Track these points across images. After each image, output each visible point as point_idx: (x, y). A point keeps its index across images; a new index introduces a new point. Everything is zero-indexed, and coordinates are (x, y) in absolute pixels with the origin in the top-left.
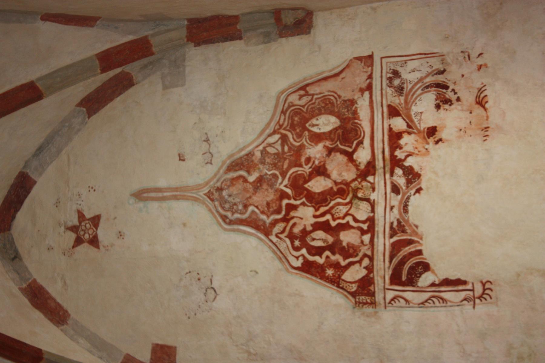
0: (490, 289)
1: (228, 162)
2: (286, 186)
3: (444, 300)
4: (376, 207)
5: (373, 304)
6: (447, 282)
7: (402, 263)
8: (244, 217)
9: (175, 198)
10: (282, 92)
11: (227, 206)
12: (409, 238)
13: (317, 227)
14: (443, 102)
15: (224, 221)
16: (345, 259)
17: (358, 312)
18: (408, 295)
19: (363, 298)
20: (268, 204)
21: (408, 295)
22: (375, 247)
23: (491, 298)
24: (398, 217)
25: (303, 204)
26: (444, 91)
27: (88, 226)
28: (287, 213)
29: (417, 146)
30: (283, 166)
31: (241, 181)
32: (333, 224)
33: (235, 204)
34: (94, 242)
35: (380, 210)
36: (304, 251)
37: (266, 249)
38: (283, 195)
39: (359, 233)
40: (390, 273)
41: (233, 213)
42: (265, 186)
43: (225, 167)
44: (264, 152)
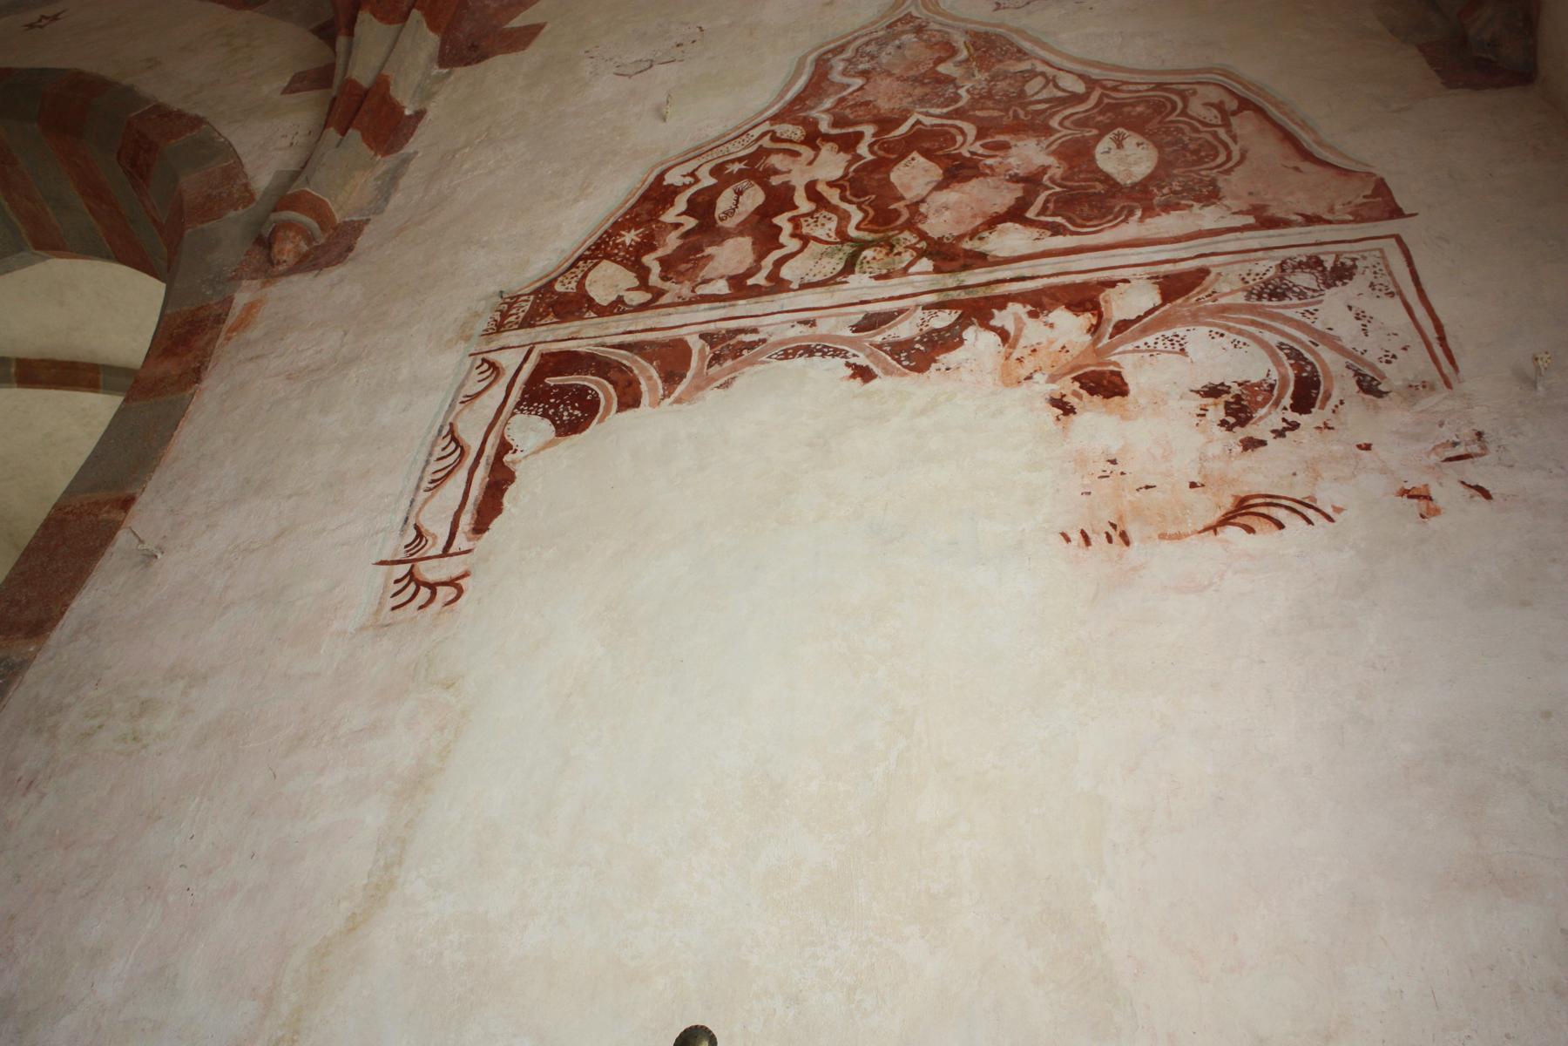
6: (500, 479)
8: (835, 76)
12: (690, 374)
26: (1287, 401)
28: (827, 138)
29: (1042, 354)
30: (982, 109)
36: (708, 181)
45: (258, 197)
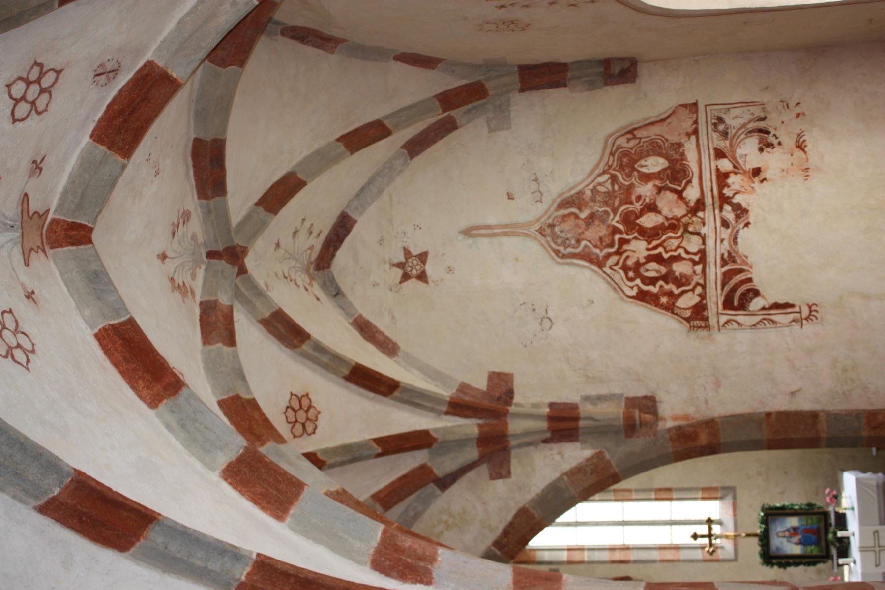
0: (816, 311)
1: (559, 200)
2: (617, 222)
3: (774, 322)
4: (707, 240)
5: (707, 327)
6: (776, 306)
7: (734, 290)
9: (506, 234)
10: (610, 136)
11: (559, 241)
12: (739, 267)
13: (649, 259)
14: (765, 145)
15: (558, 256)
16: (678, 287)
17: (693, 335)
18: (740, 319)
19: (697, 323)
20: (601, 239)
21: (740, 319)
22: (707, 275)
23: (817, 318)
24: (728, 248)
25: (635, 238)
27: (415, 262)
28: (620, 247)
31: (572, 218)
32: (666, 256)
33: (568, 239)
34: (422, 277)
35: (710, 243)
37: (600, 280)
38: (615, 230)
39: (691, 264)
40: (723, 299)
41: (566, 248)
42: (597, 222)
43: (555, 205)
44: (594, 191)
45: (597, 451)
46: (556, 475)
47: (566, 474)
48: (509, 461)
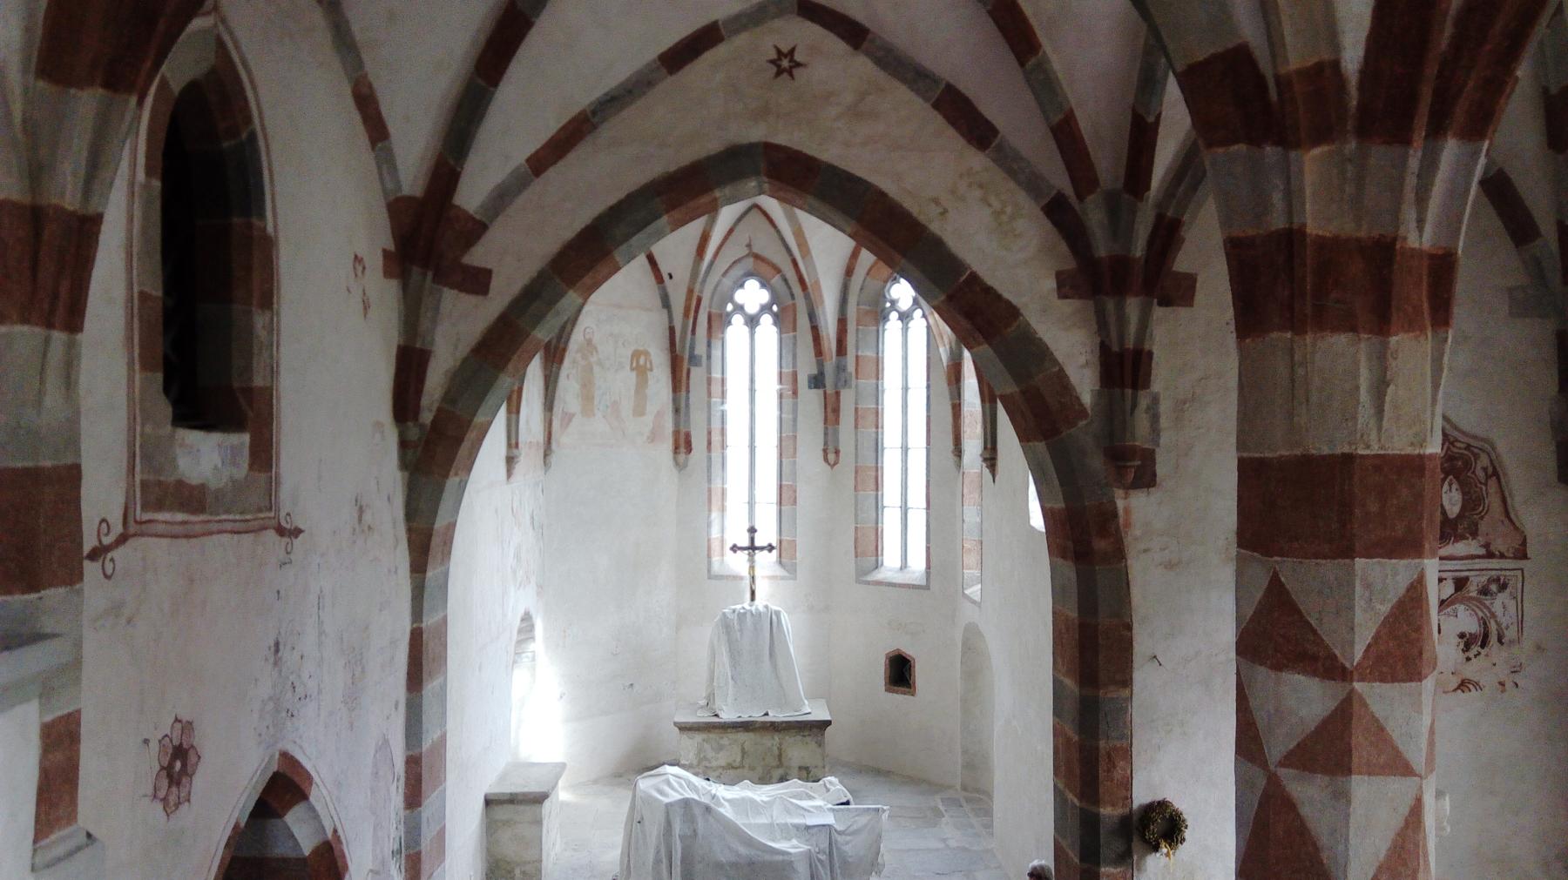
14: (1467, 641)
46: (1059, 355)
47: (1062, 370)
48: (1081, 297)
